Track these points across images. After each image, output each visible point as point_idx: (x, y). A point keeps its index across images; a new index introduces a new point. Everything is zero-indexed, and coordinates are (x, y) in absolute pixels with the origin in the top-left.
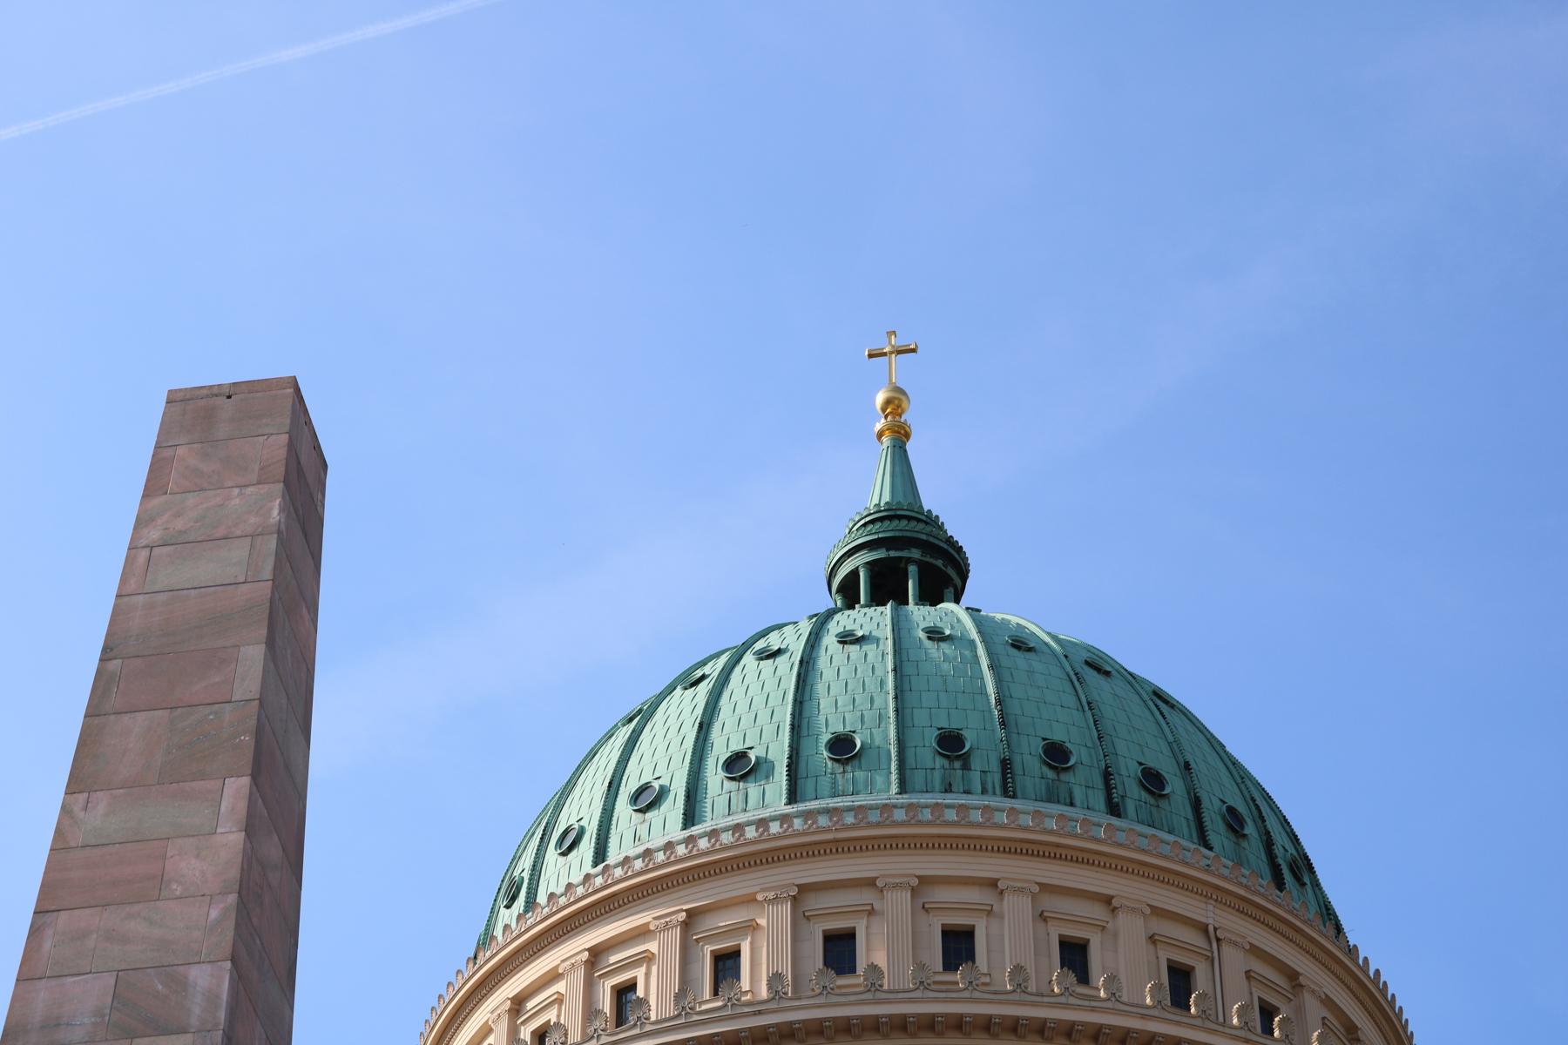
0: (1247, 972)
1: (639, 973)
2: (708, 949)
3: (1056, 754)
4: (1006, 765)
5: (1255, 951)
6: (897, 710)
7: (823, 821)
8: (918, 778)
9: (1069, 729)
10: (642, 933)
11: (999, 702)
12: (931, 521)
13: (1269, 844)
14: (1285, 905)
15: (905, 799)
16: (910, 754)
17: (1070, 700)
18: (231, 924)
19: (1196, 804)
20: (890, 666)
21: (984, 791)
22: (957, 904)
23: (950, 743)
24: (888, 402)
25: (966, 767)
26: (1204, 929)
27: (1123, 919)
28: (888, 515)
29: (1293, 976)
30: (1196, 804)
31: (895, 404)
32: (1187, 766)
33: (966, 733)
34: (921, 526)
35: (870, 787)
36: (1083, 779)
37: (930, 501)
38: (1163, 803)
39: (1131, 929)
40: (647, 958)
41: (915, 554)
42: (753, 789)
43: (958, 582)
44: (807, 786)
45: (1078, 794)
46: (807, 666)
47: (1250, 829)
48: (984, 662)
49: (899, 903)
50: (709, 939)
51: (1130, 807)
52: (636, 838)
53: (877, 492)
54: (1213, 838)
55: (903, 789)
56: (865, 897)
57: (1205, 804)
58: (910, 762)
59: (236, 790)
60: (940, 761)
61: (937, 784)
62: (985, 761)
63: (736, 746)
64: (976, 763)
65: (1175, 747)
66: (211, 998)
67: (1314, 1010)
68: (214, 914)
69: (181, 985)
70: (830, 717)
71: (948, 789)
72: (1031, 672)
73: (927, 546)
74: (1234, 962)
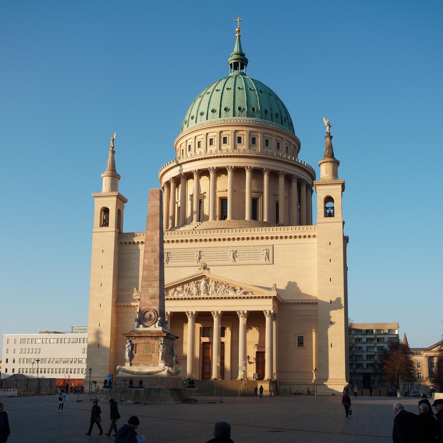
13: (281, 118)
18: (159, 243)
19: (272, 115)
20: (233, 96)
25: (242, 113)
29: (282, 138)
30: (272, 115)
32: (271, 108)
38: (267, 115)
41: (240, 61)
43: (246, 64)
44: (222, 115)
46: (222, 94)
47: (279, 116)
51: (263, 116)
52: (201, 121)
54: (274, 119)
57: (273, 114)
59: (158, 231)
60: (239, 112)
66: (158, 250)
68: (158, 243)
69: (156, 248)
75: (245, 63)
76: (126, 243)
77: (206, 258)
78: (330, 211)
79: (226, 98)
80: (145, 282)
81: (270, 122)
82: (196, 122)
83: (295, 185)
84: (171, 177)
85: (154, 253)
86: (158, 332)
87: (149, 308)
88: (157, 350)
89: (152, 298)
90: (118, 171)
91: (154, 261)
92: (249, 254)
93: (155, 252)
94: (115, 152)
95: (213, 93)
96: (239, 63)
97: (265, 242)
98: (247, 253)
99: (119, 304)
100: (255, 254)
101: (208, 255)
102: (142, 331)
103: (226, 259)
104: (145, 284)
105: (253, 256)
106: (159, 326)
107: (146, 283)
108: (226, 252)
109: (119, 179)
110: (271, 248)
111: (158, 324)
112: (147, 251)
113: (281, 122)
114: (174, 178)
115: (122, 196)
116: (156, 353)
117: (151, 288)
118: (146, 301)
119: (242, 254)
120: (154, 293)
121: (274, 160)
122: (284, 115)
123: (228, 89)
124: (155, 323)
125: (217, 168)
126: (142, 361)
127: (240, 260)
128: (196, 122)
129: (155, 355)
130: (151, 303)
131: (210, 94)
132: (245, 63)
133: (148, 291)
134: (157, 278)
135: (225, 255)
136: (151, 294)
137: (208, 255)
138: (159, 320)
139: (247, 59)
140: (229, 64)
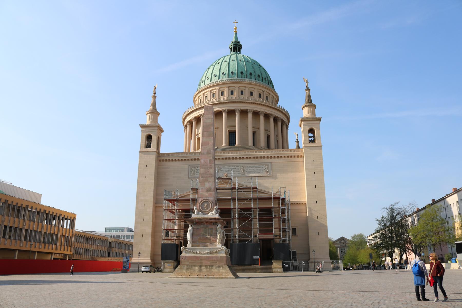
0: (266, 94)
1: (215, 93)
3: (251, 74)
4: (246, 75)
5: (266, 92)
6: (237, 69)
7: (231, 80)
8: (239, 76)
10: (215, 89)
11: (246, 68)
12: (239, 42)
13: (268, 81)
14: (270, 87)
15: (238, 79)
16: (238, 74)
17: (252, 68)
19: (262, 78)
21: (244, 78)
22: (242, 89)
23: (242, 73)
24: (235, 28)
25: (243, 75)
26: (262, 90)
27: (256, 90)
28: (235, 42)
29: (269, 93)
30: (262, 78)
31: (236, 29)
33: (243, 72)
34: (238, 43)
35: (235, 77)
36: (253, 76)
37: (239, 40)
39: (256, 90)
40: (216, 92)
41: (238, 46)
42: (225, 76)
44: (229, 76)
45: (252, 78)
46: (229, 63)
47: (267, 80)
48: (245, 64)
49: (237, 88)
50: (221, 90)
51: (257, 78)
52: (214, 80)
53: (234, 39)
54: (264, 81)
55: (238, 77)
58: (238, 74)
60: (241, 74)
61: (240, 77)
62: (245, 75)
63: (223, 72)
64: (244, 75)
65: (261, 72)
67: (271, 96)
68: (212, 146)
69: (211, 151)
70: (231, 70)
71: (241, 77)
72: (249, 65)
73: (239, 45)
74: (265, 93)
75: (241, 48)
76: (163, 160)
77: (223, 171)
78: (311, 139)
79: (232, 66)
80: (203, 178)
82: (211, 81)
83: (279, 124)
84: (193, 117)
85: (209, 155)
86: (215, 219)
87: (205, 198)
88: (214, 233)
89: (209, 190)
90: (158, 109)
91: (209, 161)
92: (255, 169)
93: (210, 154)
94: (156, 97)
95: (223, 63)
96: (237, 47)
97: (266, 160)
98: (253, 168)
99: (158, 205)
100: (259, 168)
101: (224, 170)
102: (201, 217)
103: (238, 172)
104: (202, 180)
105: (257, 170)
106: (215, 213)
107: (203, 178)
108: (238, 167)
109: (159, 115)
110: (270, 165)
111: (215, 212)
112: (204, 153)
113: (268, 83)
114: (195, 118)
115: (161, 127)
116: (214, 235)
117: (208, 183)
118: (203, 193)
119: (249, 169)
120: (210, 186)
121: (267, 106)
122: (269, 79)
123: (233, 60)
124: (212, 211)
125: (228, 110)
126: (202, 243)
127: (248, 173)
128: (211, 81)
129: (213, 238)
130: (208, 195)
131: (220, 64)
132: (241, 48)
133: (205, 185)
134: (212, 174)
135: (237, 169)
136: (207, 188)
137: (224, 170)
138: (216, 208)
139: (242, 45)
140: (230, 48)
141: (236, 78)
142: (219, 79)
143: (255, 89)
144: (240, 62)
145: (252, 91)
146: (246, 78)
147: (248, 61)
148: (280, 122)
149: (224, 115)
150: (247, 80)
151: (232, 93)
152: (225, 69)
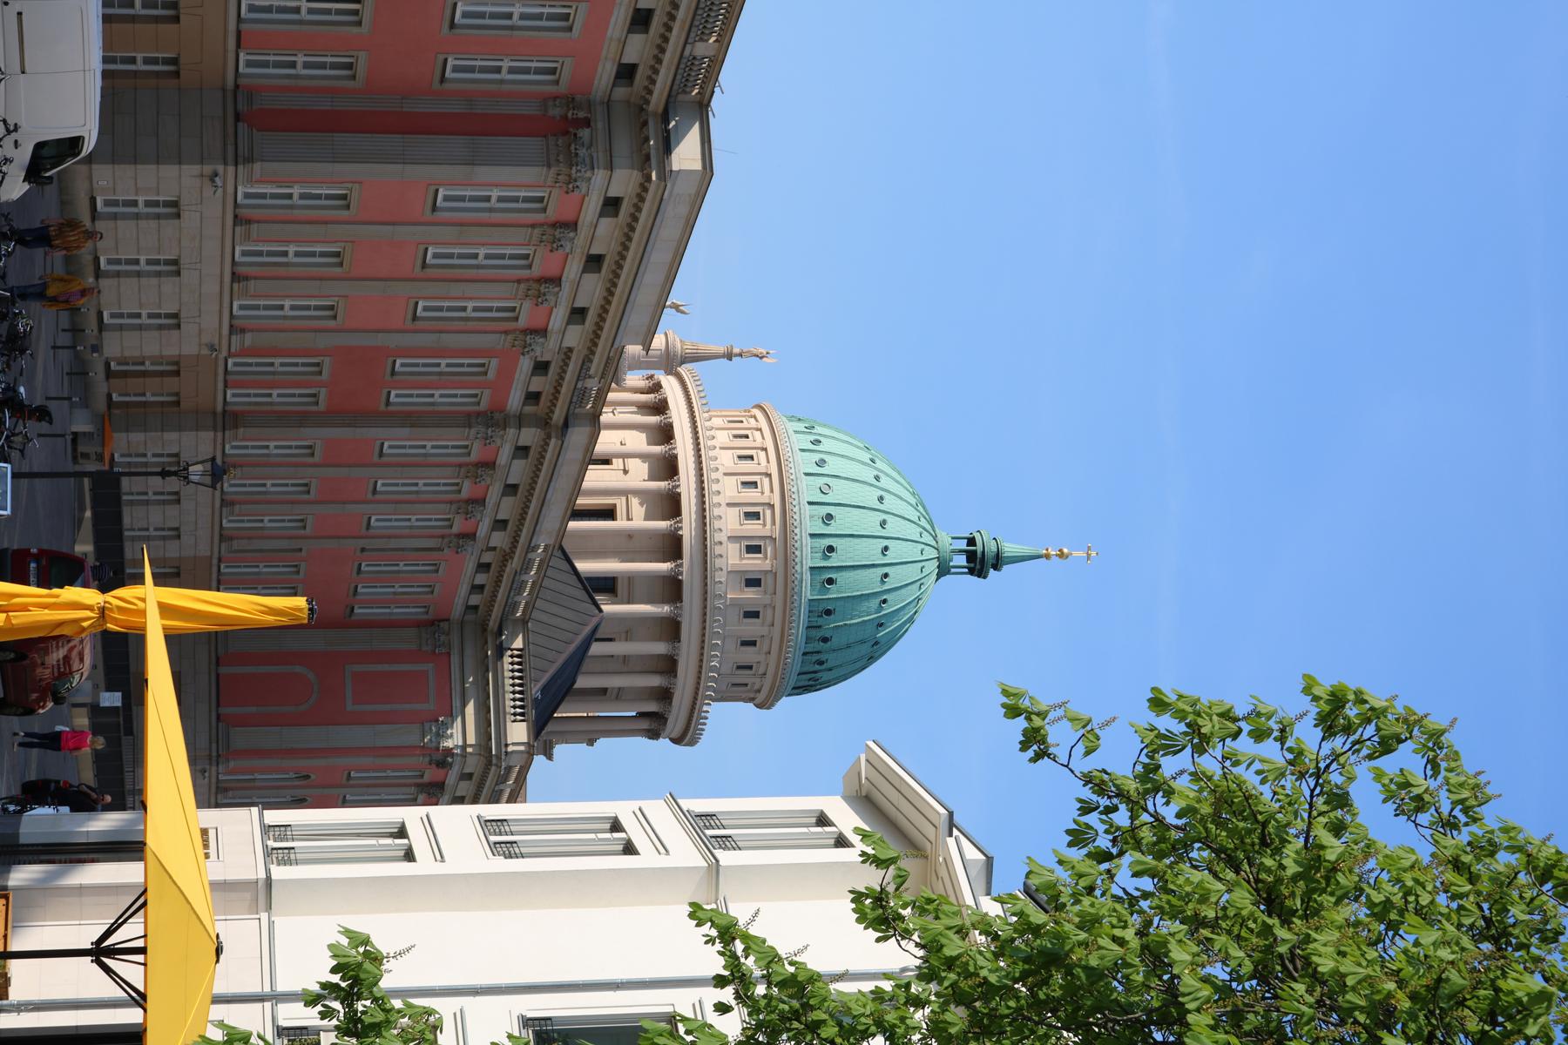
2: (762, 544)
3: (825, 640)
4: (820, 627)
8: (813, 604)
9: (834, 643)
10: (774, 523)
19: (815, 672)
22: (767, 615)
23: (828, 612)
40: (764, 525)
41: (978, 567)
44: (816, 572)
49: (767, 599)
53: (1010, 548)
54: (804, 677)
56: (770, 590)
60: (821, 609)
74: (757, 681)
81: (797, 668)
141: (807, 593)
142: (812, 535)
143: (766, 654)
144: (874, 603)
145: (758, 644)
146: (808, 627)
147: (881, 625)
148: (651, 725)
149: (665, 567)
150: (799, 630)
151: (753, 582)
152: (848, 552)
